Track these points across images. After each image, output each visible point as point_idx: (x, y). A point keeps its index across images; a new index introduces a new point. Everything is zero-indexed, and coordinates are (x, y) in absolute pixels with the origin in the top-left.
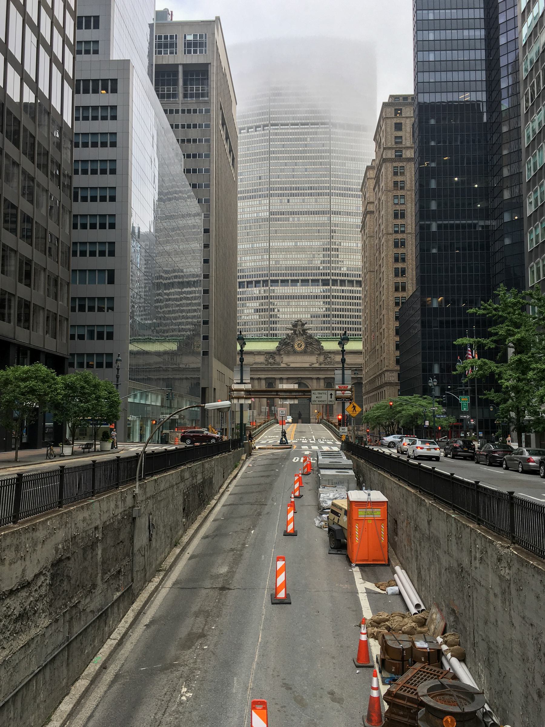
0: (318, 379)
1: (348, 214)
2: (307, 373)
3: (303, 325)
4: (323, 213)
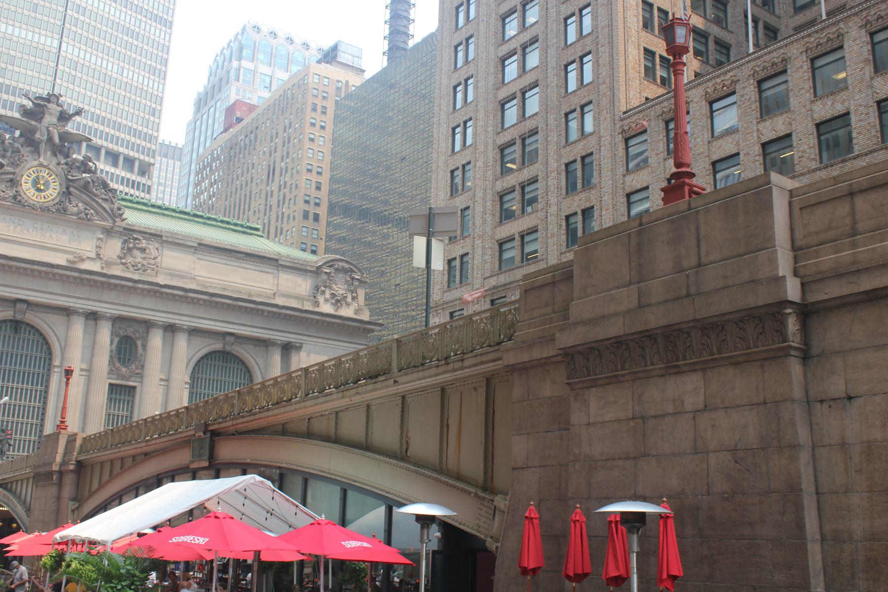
0: (93, 317)
2: (55, 287)
3: (64, 117)
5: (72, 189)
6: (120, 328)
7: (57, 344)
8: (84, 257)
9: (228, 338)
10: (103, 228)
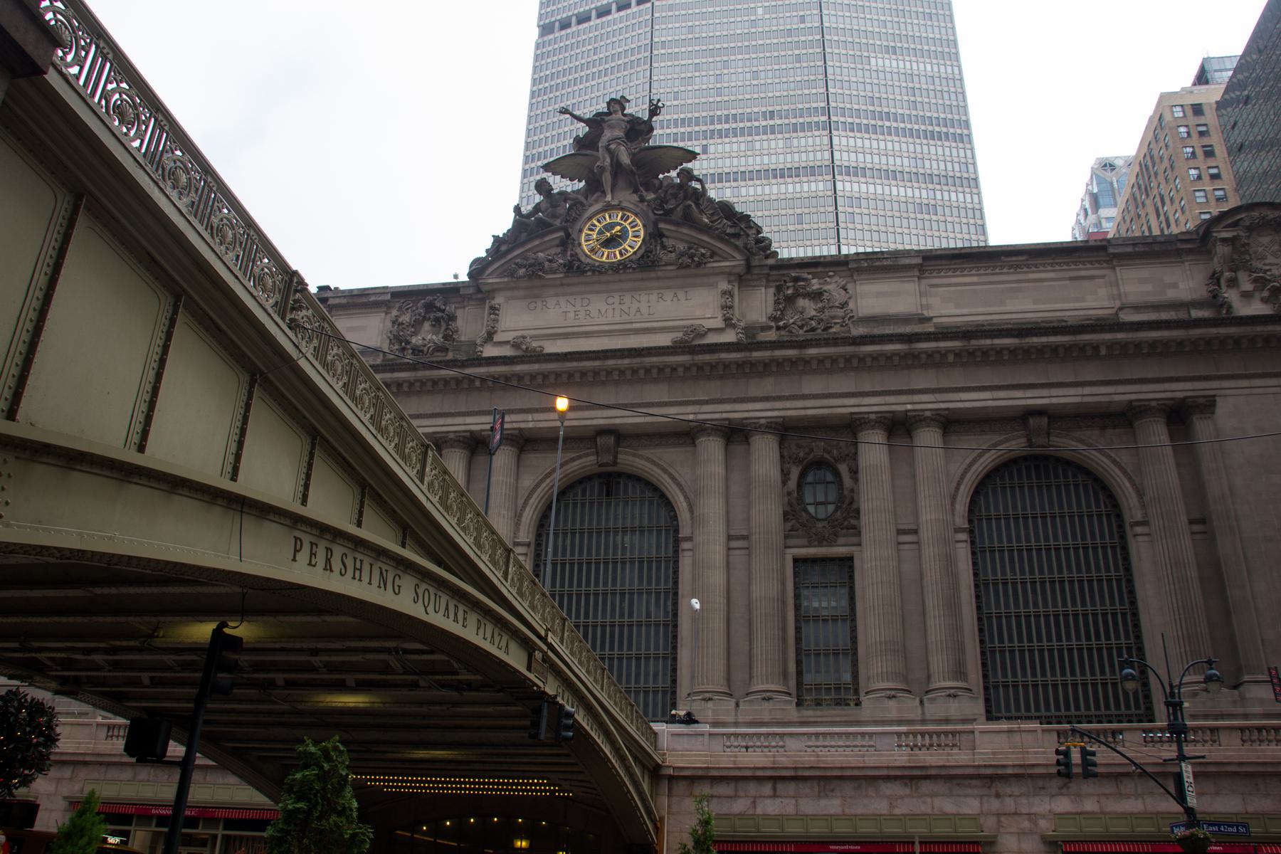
1: (891, 175)
3: (638, 130)
4: (812, 171)
5: (662, 225)
6: (799, 446)
7: (682, 498)
8: (701, 330)
9: (1032, 422)
10: (730, 274)
